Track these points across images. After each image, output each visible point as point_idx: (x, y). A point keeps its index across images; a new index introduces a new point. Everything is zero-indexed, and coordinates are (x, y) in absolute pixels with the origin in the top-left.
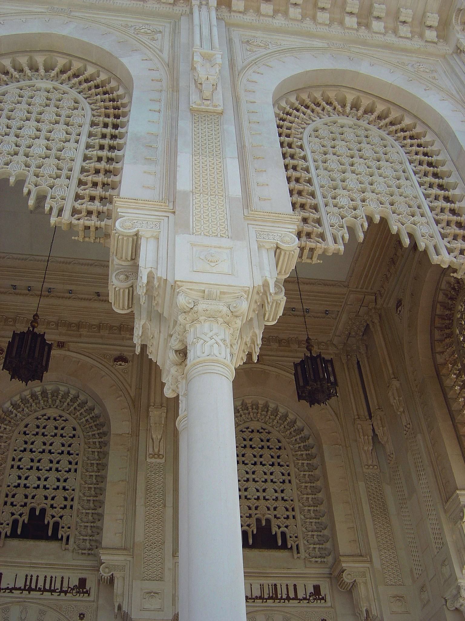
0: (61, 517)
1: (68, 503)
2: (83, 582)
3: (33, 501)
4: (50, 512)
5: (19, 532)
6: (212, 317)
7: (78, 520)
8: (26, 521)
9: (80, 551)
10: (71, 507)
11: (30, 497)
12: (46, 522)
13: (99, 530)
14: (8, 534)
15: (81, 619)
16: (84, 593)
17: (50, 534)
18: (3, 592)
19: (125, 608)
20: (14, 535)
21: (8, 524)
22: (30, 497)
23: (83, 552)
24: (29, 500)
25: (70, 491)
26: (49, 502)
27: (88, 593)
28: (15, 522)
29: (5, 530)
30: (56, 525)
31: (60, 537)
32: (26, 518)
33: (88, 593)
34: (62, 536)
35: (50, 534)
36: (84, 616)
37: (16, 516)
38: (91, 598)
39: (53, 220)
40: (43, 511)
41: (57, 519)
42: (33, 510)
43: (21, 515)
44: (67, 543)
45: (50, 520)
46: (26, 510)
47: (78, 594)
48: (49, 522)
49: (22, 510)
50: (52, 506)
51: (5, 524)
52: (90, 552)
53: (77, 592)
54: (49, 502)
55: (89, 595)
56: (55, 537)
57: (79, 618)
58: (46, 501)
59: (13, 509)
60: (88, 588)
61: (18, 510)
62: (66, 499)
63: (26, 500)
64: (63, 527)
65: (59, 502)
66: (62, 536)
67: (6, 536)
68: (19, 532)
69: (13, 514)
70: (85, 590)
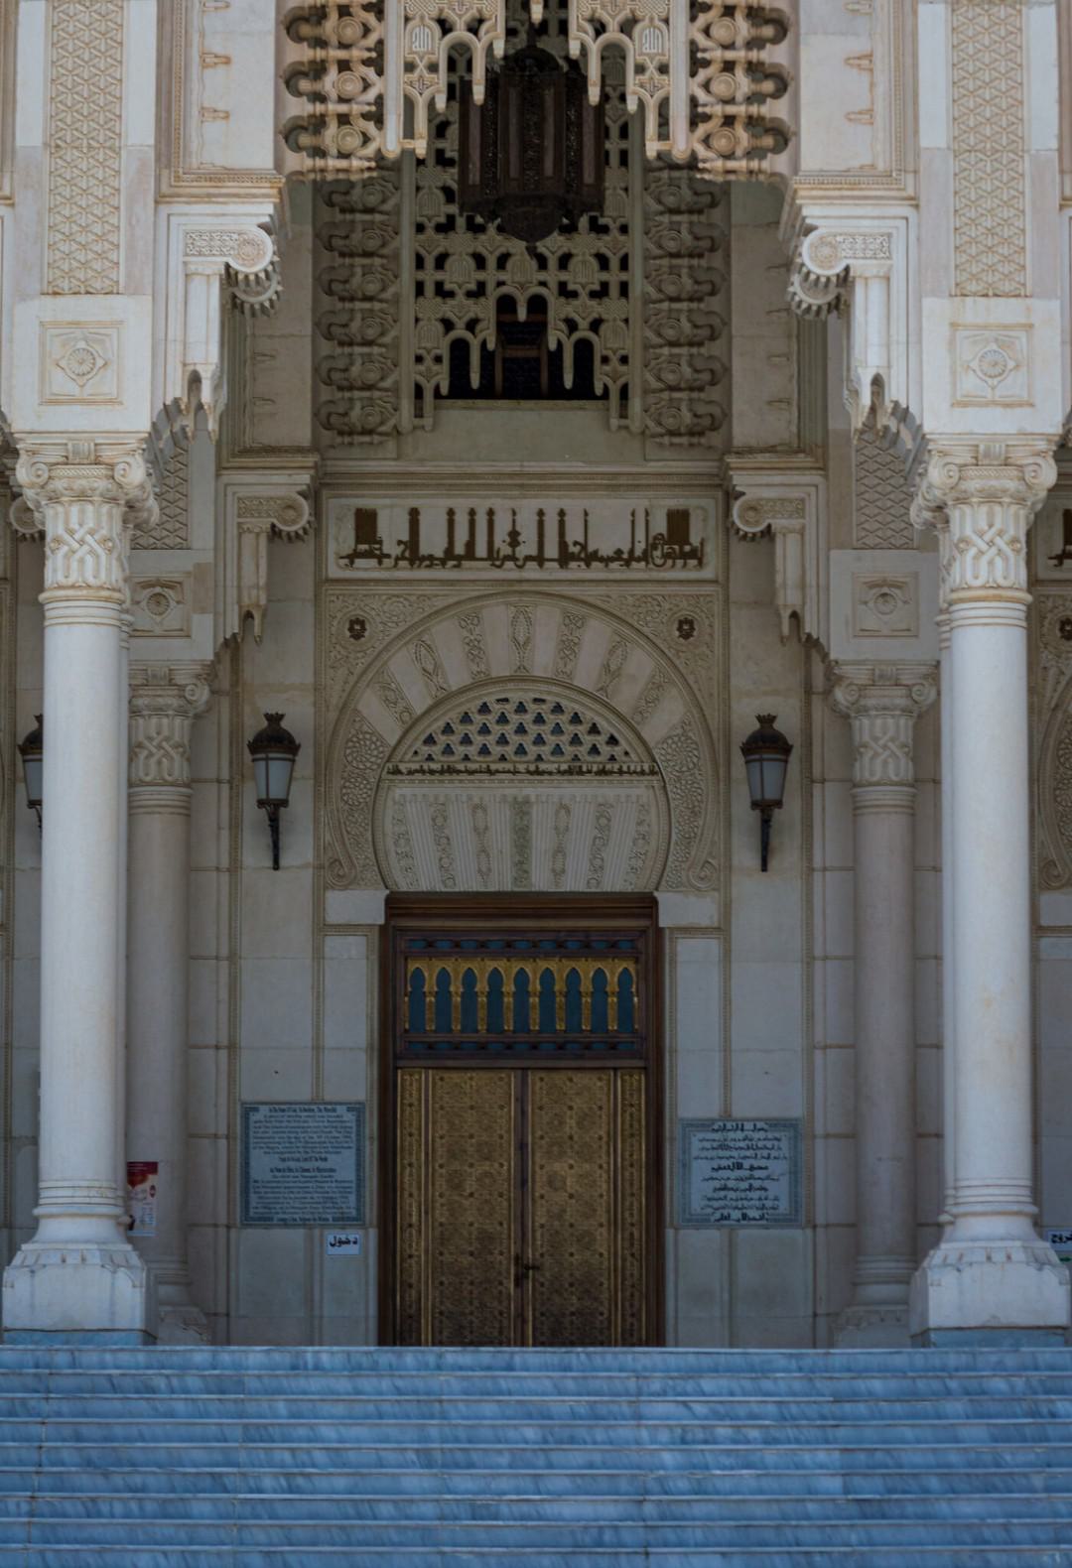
0: (596, 325)
1: (614, 277)
2: (679, 521)
3: (502, 276)
4: (558, 308)
5: (475, 381)
6: (991, 497)
7: (650, 334)
8: (491, 346)
9: (666, 440)
10: (624, 289)
11: (491, 262)
12: (553, 346)
13: (719, 376)
14: (444, 390)
15: (686, 635)
16: (685, 556)
17: (568, 381)
18: (455, 566)
19: (810, 626)
20: (460, 389)
21: (438, 359)
22: (491, 262)
23: (676, 440)
24: (491, 275)
25: (615, 232)
26: (553, 276)
27: (697, 555)
28: (460, 349)
29: (433, 382)
30: (584, 349)
31: (599, 390)
32: (488, 333)
33: (697, 555)
34: (606, 388)
35: (568, 381)
36: (692, 629)
37: (460, 332)
38: (707, 573)
39: (652, 148)
40: (538, 304)
41: (583, 332)
42: (506, 304)
43: (471, 325)
44: (623, 415)
45: (564, 338)
46: (487, 310)
47: (670, 562)
48: (560, 344)
49: (474, 309)
50: (562, 286)
51: (429, 360)
52: (695, 440)
53: (666, 556)
54: (553, 276)
55: (700, 563)
56: (583, 390)
57: (677, 633)
58: (542, 276)
59: (448, 309)
60: (695, 540)
61: (460, 309)
62: (603, 262)
63: (481, 276)
64: (605, 360)
65: (584, 275)
66: (606, 388)
67: (437, 394)
68: (475, 381)
69: (448, 325)
70: (687, 548)
